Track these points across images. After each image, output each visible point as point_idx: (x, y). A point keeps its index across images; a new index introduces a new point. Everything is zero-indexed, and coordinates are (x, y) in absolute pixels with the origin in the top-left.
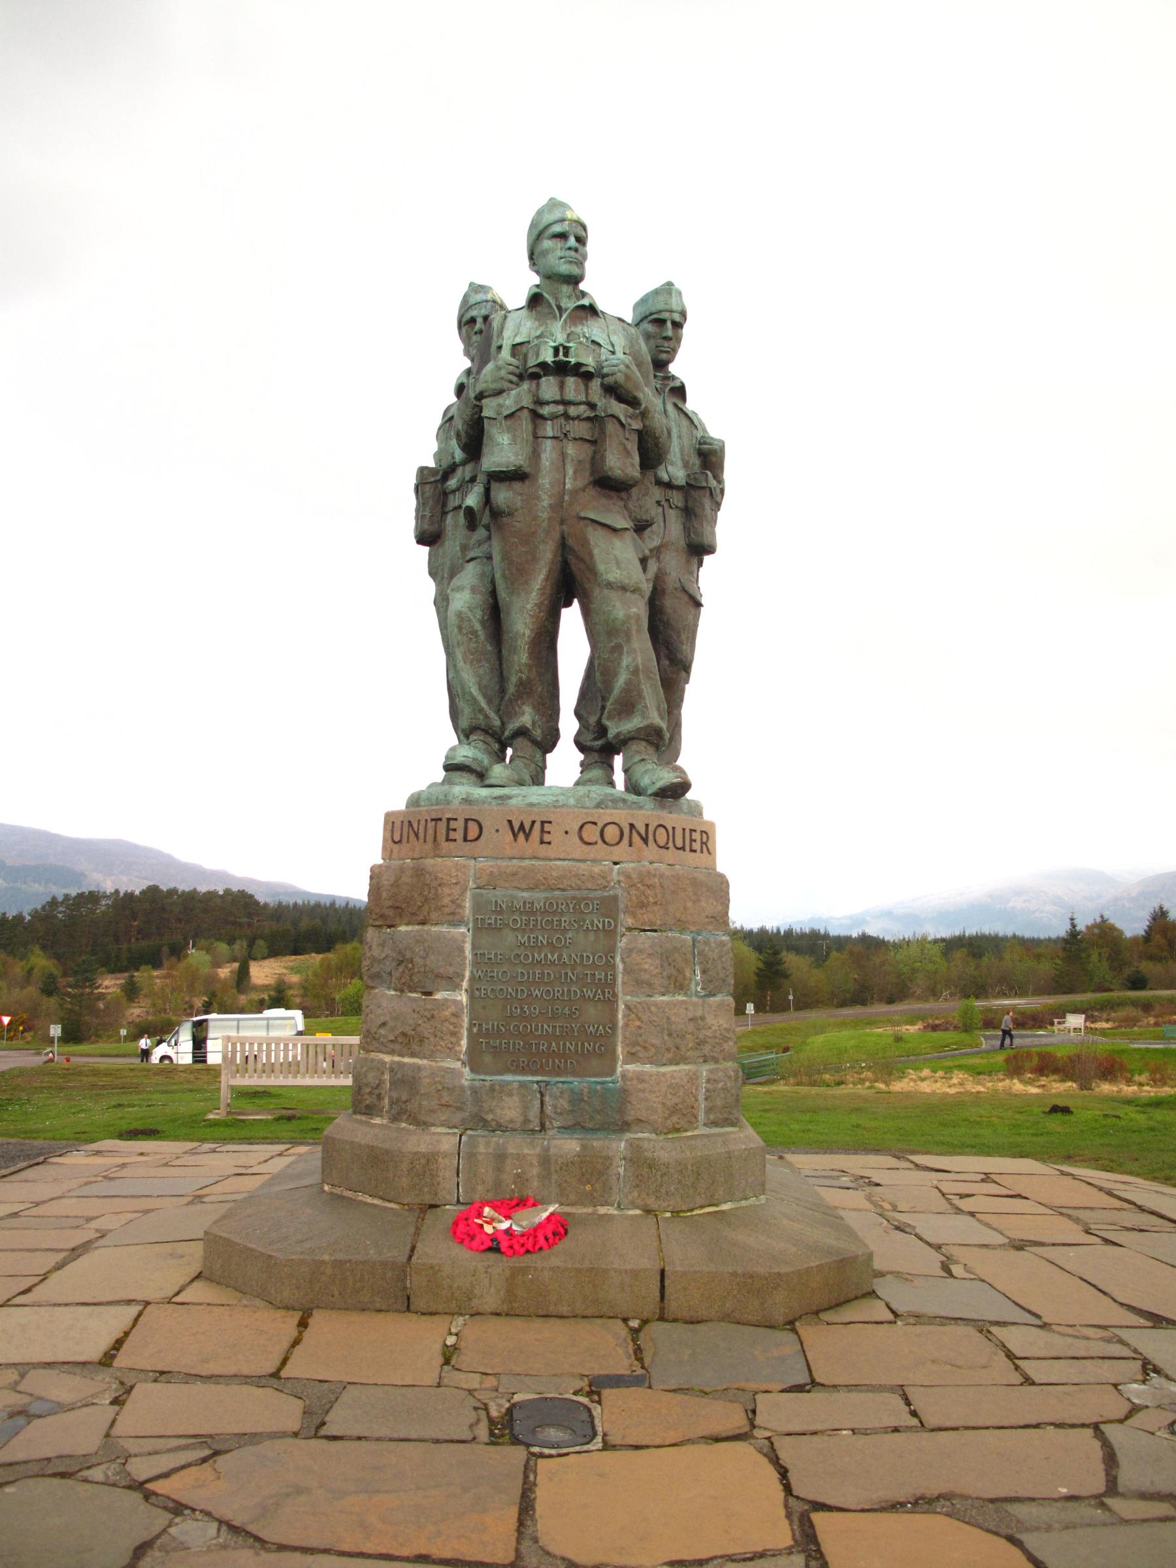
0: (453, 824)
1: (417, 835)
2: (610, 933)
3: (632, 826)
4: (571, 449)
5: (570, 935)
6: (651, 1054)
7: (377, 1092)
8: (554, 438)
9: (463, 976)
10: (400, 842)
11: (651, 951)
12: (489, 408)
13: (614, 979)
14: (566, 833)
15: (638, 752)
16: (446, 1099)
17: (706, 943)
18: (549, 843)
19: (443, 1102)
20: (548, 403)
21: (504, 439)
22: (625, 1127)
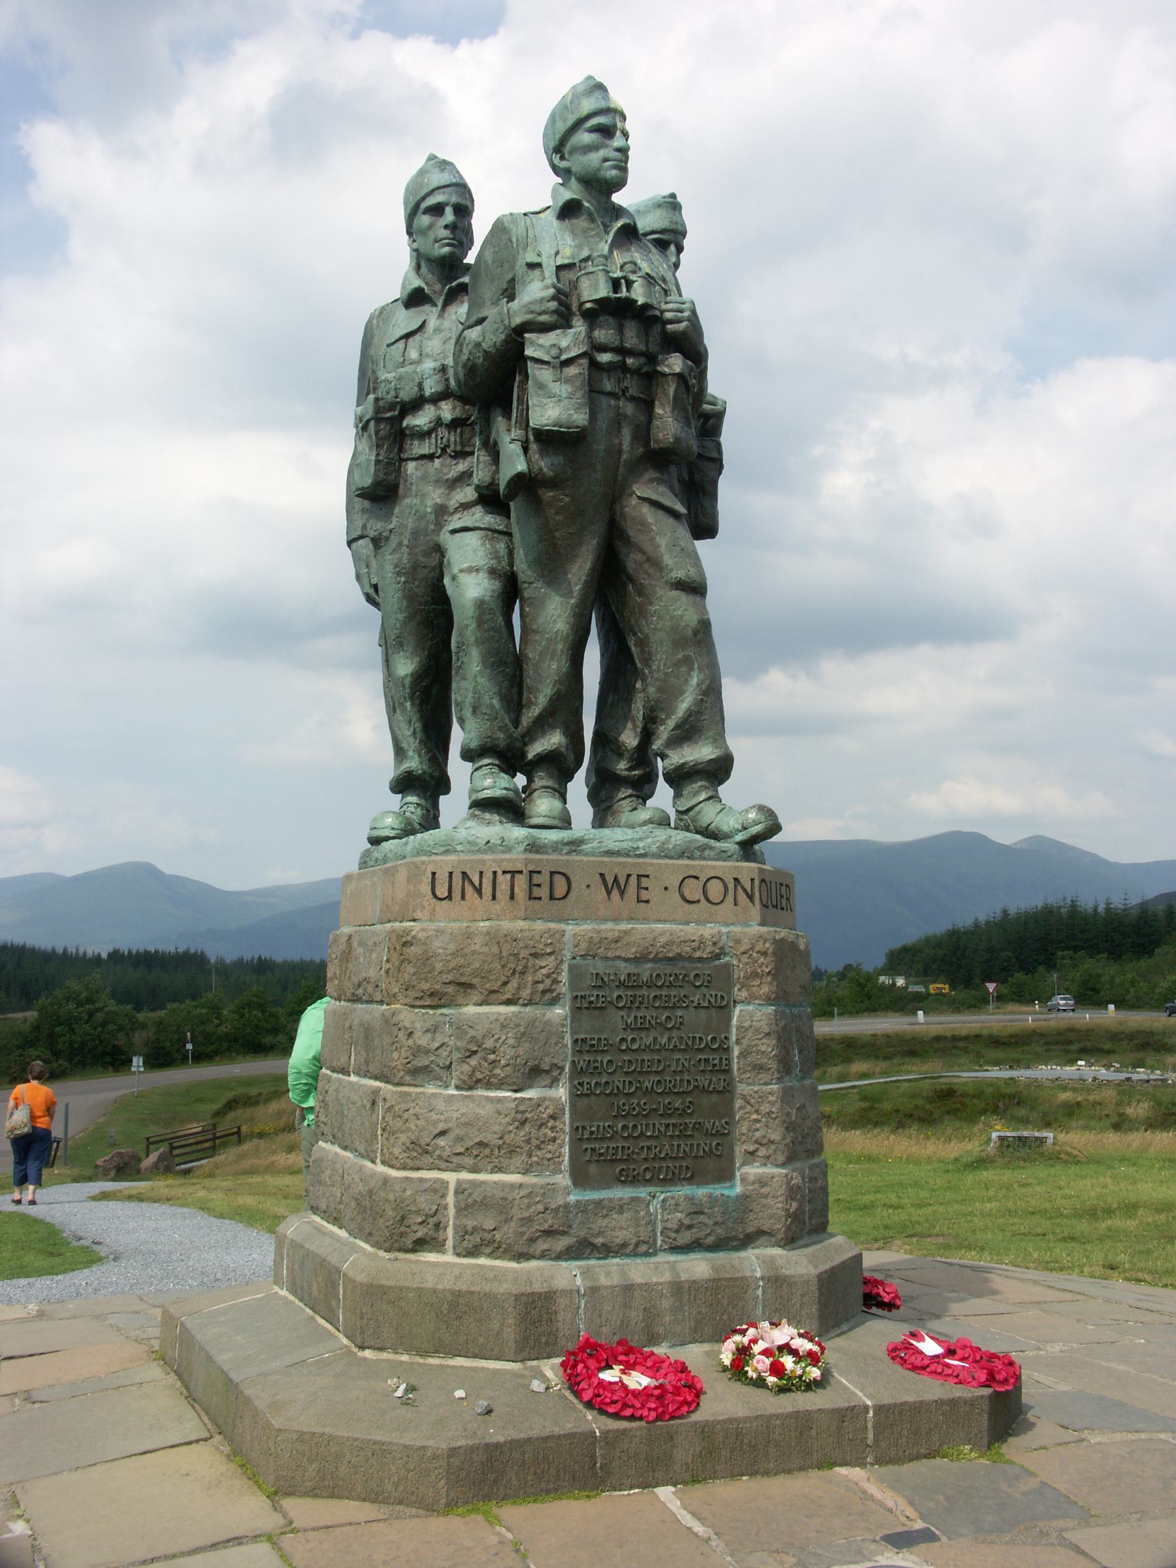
0: (536, 879)
1: (479, 891)
2: (724, 1009)
3: (736, 879)
4: (629, 409)
5: (679, 1013)
6: (771, 1152)
7: (432, 1221)
8: (612, 395)
9: (562, 1069)
10: (449, 897)
11: (767, 1030)
12: (537, 346)
13: (729, 1064)
14: (666, 888)
15: (706, 788)
16: (549, 1222)
17: (800, 1017)
18: (647, 902)
19: (546, 1226)
20: (603, 349)
21: (563, 389)
22: (747, 1241)
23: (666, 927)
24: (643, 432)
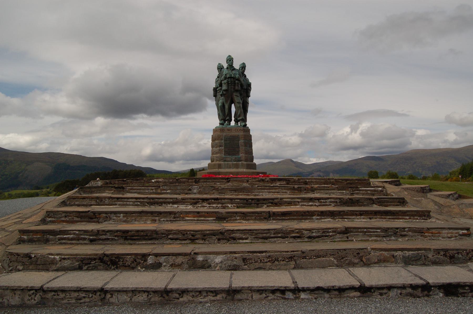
2: (239, 140)
12: (223, 82)
22: (241, 161)
23: (234, 133)
24: (234, 88)
